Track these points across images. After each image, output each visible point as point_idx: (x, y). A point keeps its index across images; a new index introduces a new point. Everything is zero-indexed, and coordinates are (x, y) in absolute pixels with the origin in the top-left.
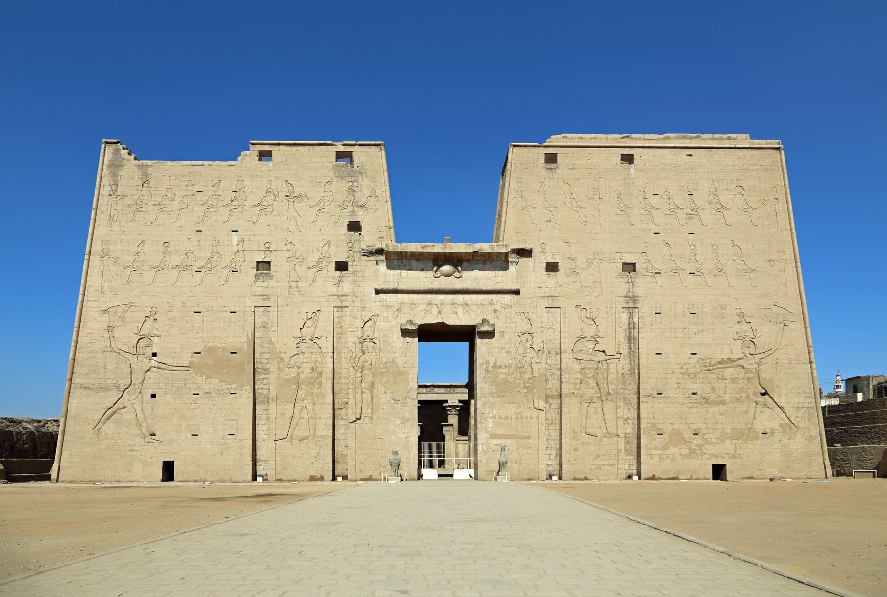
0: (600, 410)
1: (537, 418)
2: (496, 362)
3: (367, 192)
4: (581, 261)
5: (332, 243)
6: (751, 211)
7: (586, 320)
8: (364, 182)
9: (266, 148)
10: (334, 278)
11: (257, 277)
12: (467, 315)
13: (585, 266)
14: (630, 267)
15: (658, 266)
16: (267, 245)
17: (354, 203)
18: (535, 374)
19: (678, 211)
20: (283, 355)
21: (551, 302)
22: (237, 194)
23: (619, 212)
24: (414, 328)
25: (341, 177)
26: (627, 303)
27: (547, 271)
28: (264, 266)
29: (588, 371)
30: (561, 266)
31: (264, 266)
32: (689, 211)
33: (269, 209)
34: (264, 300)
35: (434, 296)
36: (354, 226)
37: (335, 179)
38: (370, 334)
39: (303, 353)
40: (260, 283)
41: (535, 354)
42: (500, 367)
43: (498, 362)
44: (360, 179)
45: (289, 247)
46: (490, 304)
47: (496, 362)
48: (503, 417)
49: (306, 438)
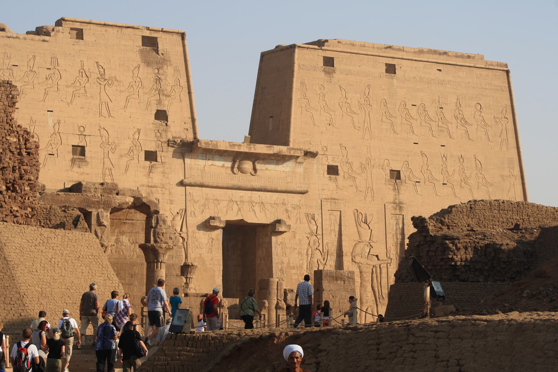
2: (289, 263)
4: (356, 166)
6: (488, 128)
7: (363, 225)
8: (169, 70)
9: (78, 26)
11: (73, 161)
14: (396, 175)
17: (160, 92)
19: (433, 124)
22: (51, 72)
24: (222, 225)
25: (148, 64)
26: (395, 209)
27: (328, 174)
28: (80, 151)
29: (365, 275)
32: (440, 124)
36: (161, 115)
37: (142, 65)
40: (76, 169)
42: (293, 268)
43: (291, 262)
44: (165, 67)
45: (104, 133)
47: (289, 263)
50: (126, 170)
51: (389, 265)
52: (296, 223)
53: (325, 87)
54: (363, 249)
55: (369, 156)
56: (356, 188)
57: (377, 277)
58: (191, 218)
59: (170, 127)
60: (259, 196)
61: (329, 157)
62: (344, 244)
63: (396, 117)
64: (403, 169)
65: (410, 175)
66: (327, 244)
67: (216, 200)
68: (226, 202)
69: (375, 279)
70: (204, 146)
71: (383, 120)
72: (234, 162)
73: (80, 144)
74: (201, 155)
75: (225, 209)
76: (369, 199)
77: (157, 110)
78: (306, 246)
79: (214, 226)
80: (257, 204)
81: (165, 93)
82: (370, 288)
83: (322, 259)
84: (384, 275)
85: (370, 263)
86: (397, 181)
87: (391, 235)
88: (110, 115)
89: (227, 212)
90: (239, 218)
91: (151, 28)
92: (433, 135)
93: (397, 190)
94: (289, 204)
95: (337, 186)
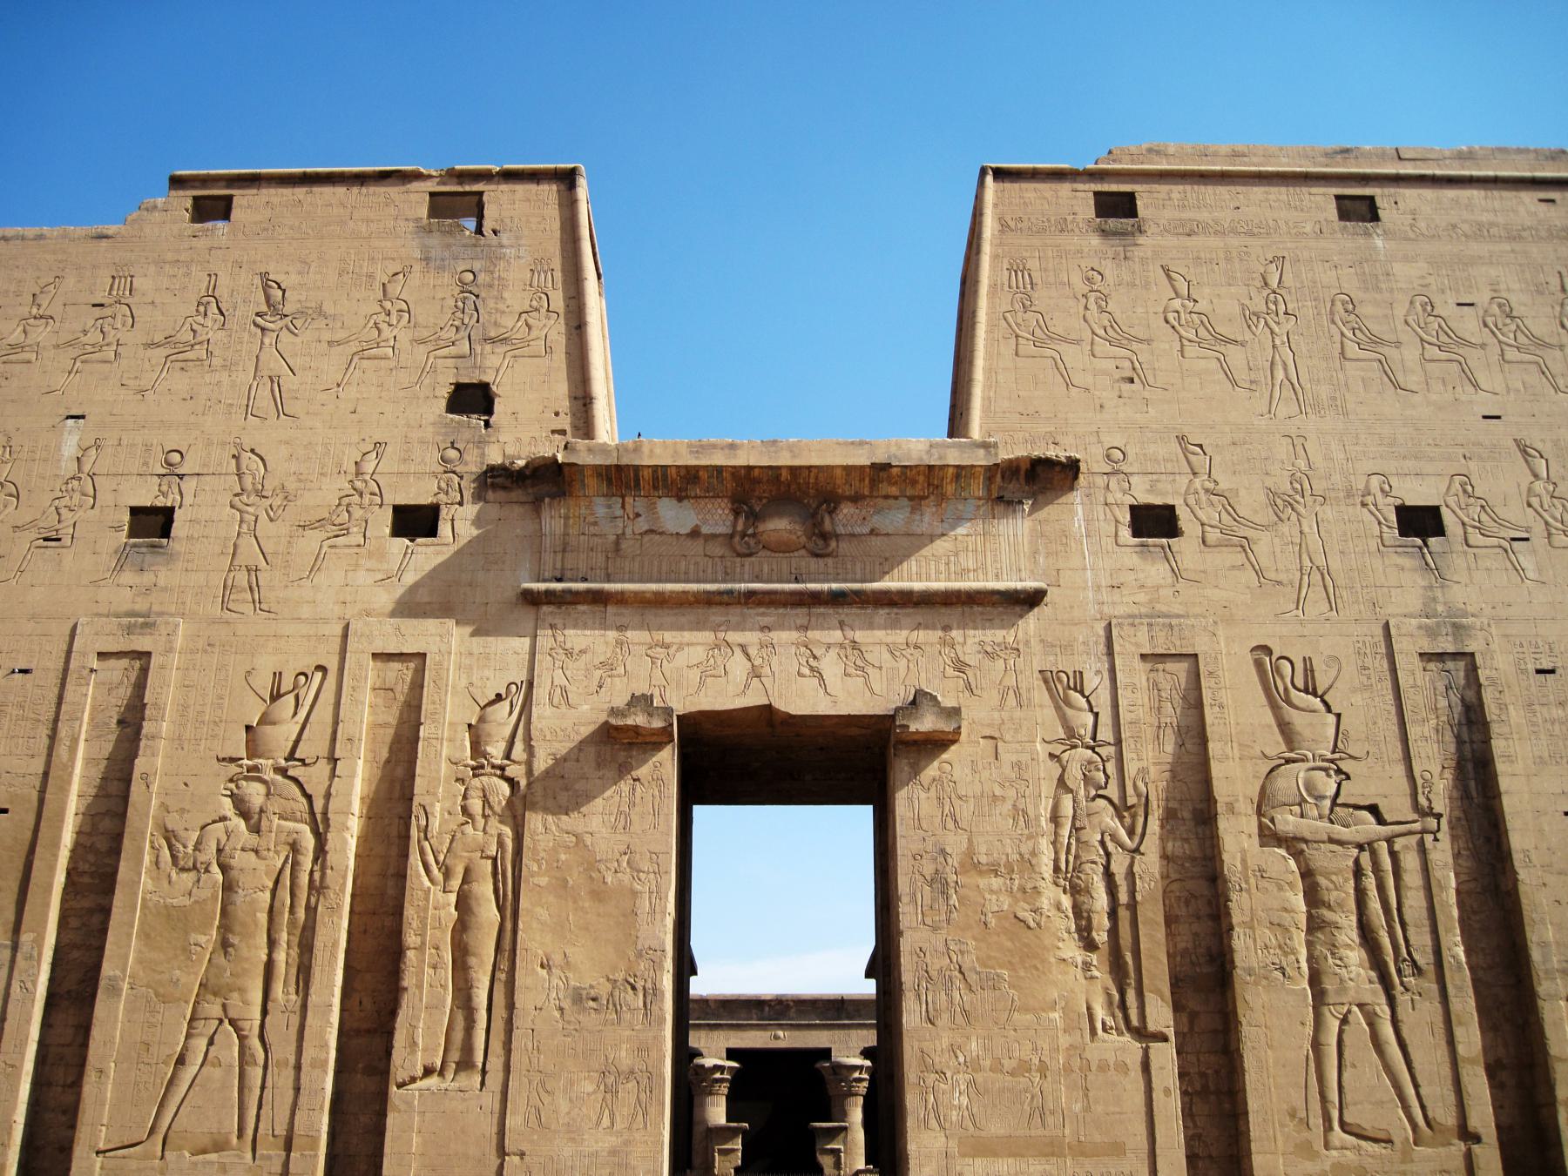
0: (1387, 1031)
1: (1146, 1066)
2: (970, 852)
3: (516, 299)
4: (1251, 503)
5: (389, 449)
7: (1299, 697)
11: (122, 559)
13: (1266, 516)
14: (1420, 523)
15: (1515, 512)
16: (176, 457)
18: (1123, 897)
20: (173, 822)
22: (107, 311)
23: (1352, 349)
24: (658, 723)
26: (1432, 633)
27: (1135, 535)
28: (153, 523)
29: (1322, 881)
31: (153, 523)
34: (130, 630)
36: (473, 399)
37: (417, 267)
39: (244, 814)
40: (128, 577)
41: (1115, 824)
43: (983, 849)
47: (970, 852)
48: (1008, 1064)
49: (219, 1146)
51: (1429, 838)
52: (1002, 707)
53: (1107, 273)
54: (1310, 787)
55: (1302, 464)
56: (1259, 573)
57: (1381, 887)
58: (549, 711)
59: (498, 430)
61: (1134, 480)
62: (1216, 770)
64: (1452, 501)
65: (1484, 517)
66: (1143, 771)
68: (700, 649)
69: (1373, 893)
70: (584, 458)
71: (1349, 355)
72: (736, 513)
73: (161, 502)
74: (600, 501)
75: (695, 675)
76: (1316, 605)
77: (459, 387)
78: (1048, 788)
79: (627, 728)
80: (833, 652)
81: (493, 334)
82: (1355, 935)
83: (1123, 834)
84: (1412, 878)
85: (1339, 831)
86: (1432, 541)
87: (1428, 729)
88: (281, 411)
89: (702, 683)
90: (753, 699)
91: (458, 167)
92: (1557, 389)
93: (1435, 571)
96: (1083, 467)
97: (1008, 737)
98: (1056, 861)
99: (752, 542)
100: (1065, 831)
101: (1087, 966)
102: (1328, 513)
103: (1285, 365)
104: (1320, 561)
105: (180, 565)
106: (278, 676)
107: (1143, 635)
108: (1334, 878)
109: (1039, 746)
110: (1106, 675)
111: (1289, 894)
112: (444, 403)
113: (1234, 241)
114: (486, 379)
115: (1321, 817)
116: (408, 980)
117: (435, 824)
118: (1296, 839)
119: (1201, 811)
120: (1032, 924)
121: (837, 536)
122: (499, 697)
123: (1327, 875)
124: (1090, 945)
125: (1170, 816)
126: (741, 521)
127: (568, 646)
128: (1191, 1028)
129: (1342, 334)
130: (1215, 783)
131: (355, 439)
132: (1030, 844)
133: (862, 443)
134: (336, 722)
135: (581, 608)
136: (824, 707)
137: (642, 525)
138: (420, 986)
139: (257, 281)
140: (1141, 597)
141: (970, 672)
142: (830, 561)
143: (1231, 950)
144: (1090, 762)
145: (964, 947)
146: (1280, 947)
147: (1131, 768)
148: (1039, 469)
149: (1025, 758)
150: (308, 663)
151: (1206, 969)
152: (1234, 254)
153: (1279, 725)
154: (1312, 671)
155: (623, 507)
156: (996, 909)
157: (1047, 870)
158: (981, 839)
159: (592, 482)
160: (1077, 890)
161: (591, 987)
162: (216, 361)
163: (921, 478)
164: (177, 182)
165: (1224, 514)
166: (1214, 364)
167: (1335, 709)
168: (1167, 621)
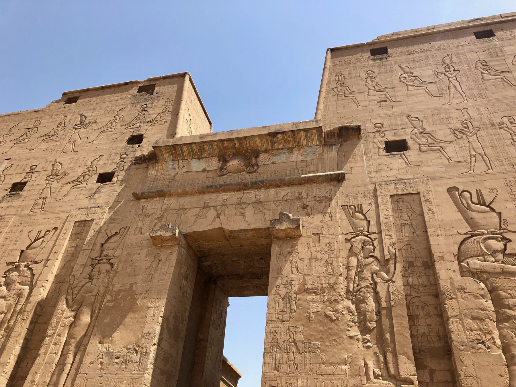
10: (90, 190)
12: (260, 216)
18: (384, 304)
21: (400, 186)
22: (30, 130)
25: (137, 103)
28: (17, 187)
29: (503, 294)
30: (410, 143)
31: (17, 187)
33: (55, 137)
35: (214, 196)
38: (111, 252)
42: (314, 291)
44: (156, 101)
46: (298, 198)
50: (65, 196)
53: (375, 71)
56: (449, 159)
60: (256, 195)
62: (432, 241)
63: (510, 72)
66: (393, 244)
67: (183, 209)
68: (198, 209)
71: (486, 78)
72: (219, 161)
74: (171, 163)
78: (344, 254)
80: (250, 206)
81: (148, 120)
94: (310, 197)
95: (408, 164)
96: (362, 128)
97: (325, 233)
98: (348, 287)
99: (225, 171)
100: (353, 273)
101: (365, 341)
102: (482, 133)
103: (455, 87)
104: (481, 151)
105: (21, 199)
106: (40, 232)
107: (392, 187)
108: (510, 291)
109: (340, 236)
110: (373, 205)
111: (483, 300)
112: (126, 142)
113: (428, 53)
114: (141, 133)
115: (497, 261)
116: (42, 351)
117: (76, 282)
118: (483, 272)
119: (427, 262)
120: (334, 318)
121: (258, 166)
122: (116, 233)
123: (505, 290)
124: (364, 330)
125: (409, 266)
126: (221, 163)
127: (147, 213)
128: (432, 380)
129: (482, 73)
130: (432, 246)
131: (94, 155)
132: (334, 278)
133: (266, 127)
134: (53, 247)
135: (155, 199)
136: (244, 226)
137: (184, 170)
138: (45, 354)
139: (79, 116)
140: (391, 173)
141: (309, 209)
142: (254, 174)
143: (450, 332)
144: (364, 240)
145: (296, 330)
146: (480, 330)
147: (387, 243)
148: (343, 132)
149: (331, 241)
150: (50, 227)
151: (437, 345)
152: (430, 57)
153: (466, 220)
154: (482, 195)
155: (178, 164)
156: (315, 310)
157: (343, 292)
158: (309, 278)
159: (167, 156)
160: (359, 302)
161: (119, 352)
162: (58, 139)
163: (291, 139)
164: (64, 94)
165: (429, 139)
166: (422, 91)
167: (497, 211)
168: (404, 181)
